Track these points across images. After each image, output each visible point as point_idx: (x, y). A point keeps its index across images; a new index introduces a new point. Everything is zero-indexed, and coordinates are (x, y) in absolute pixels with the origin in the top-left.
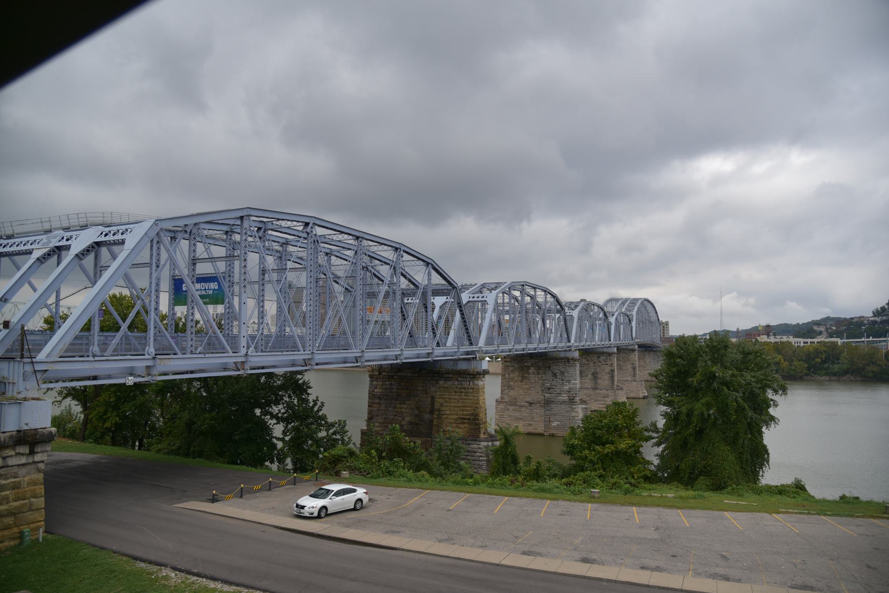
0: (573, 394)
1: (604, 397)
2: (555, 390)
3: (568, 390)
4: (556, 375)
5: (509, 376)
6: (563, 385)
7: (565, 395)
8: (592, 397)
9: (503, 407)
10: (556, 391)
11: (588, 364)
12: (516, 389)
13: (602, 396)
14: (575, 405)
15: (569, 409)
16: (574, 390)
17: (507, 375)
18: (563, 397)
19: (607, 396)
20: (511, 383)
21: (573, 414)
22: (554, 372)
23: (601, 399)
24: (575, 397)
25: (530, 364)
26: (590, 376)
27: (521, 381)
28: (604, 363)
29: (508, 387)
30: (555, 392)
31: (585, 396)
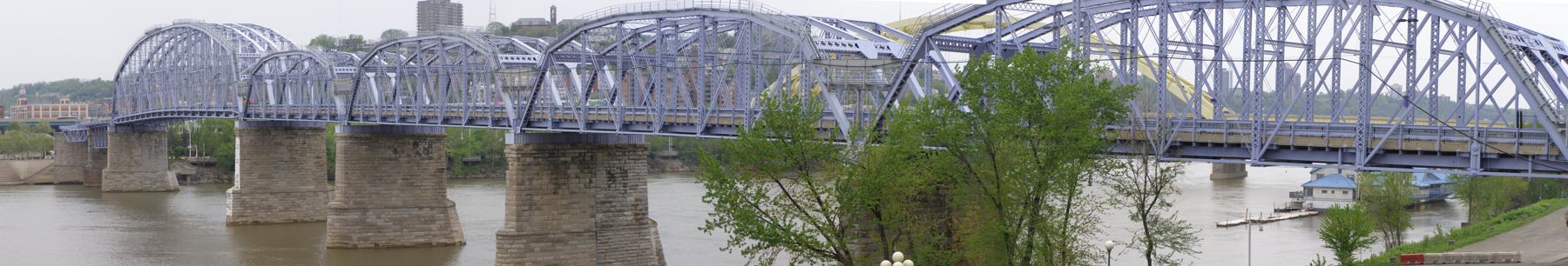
0: (641, 210)
1: (426, 222)
2: (613, 204)
3: (634, 203)
4: (614, 177)
5: (531, 184)
6: (625, 195)
7: (630, 213)
8: (405, 224)
9: (522, 246)
10: (614, 206)
11: (396, 159)
12: (545, 208)
13: (422, 220)
14: (645, 228)
15: (636, 237)
16: (643, 202)
17: (527, 183)
18: (625, 216)
19: (432, 220)
20: (536, 198)
21: (643, 246)
22: (612, 172)
23: (421, 226)
24: (644, 214)
25: (569, 159)
26: (400, 181)
27: (554, 193)
28: (423, 155)
29: (531, 205)
30: (613, 209)
31: (391, 223)
